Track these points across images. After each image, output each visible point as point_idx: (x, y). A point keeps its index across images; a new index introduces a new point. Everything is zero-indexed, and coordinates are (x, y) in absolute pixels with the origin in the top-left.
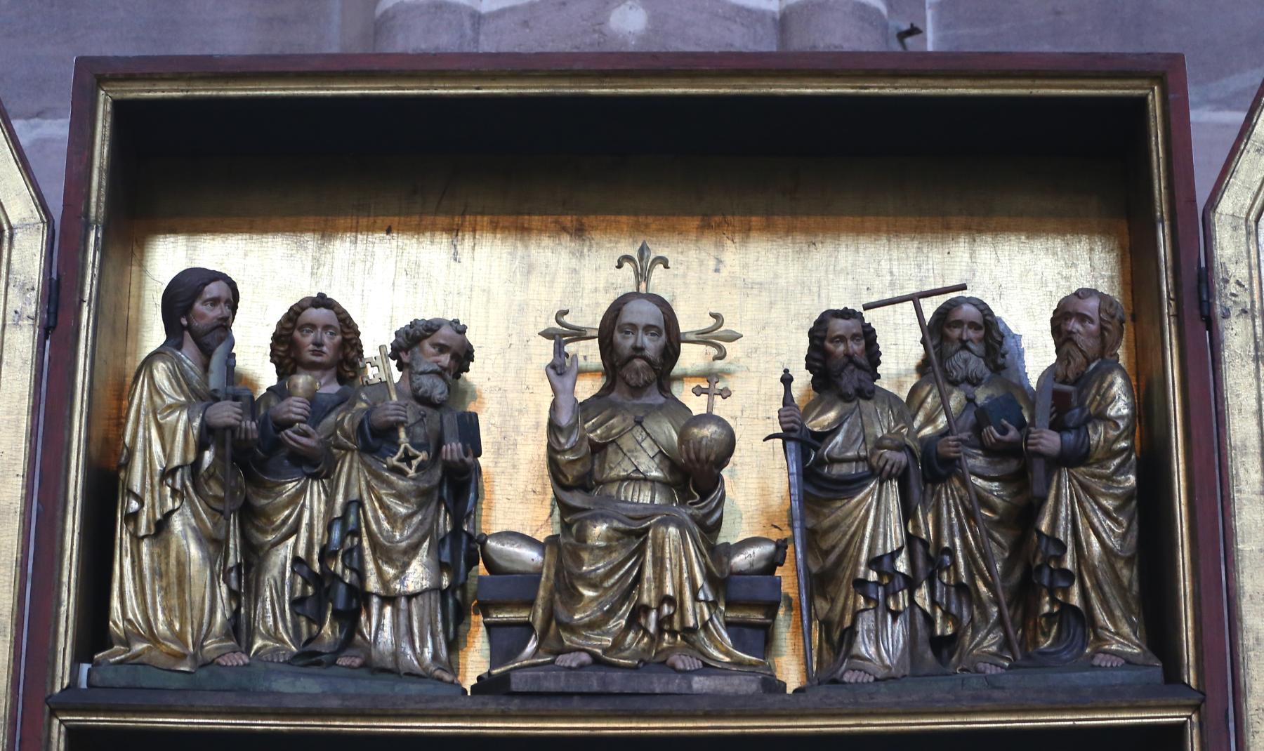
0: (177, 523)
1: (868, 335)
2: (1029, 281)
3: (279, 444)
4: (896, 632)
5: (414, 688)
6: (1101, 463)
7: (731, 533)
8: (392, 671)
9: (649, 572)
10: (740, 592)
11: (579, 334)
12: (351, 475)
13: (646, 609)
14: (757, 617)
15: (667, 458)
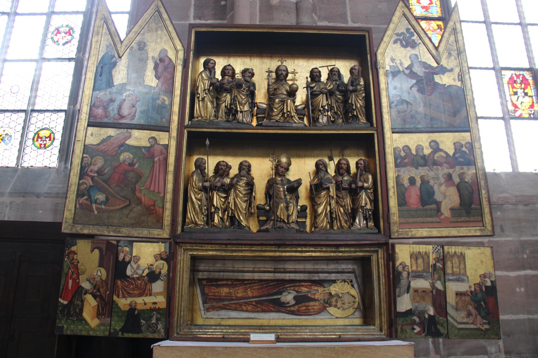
0: (206, 99)
1: (320, 72)
2: (345, 67)
3: (223, 87)
4: (325, 119)
5: (246, 125)
6: (359, 92)
7: (297, 103)
8: (243, 123)
9: (285, 107)
10: (299, 112)
11: (272, 72)
12: (235, 92)
13: (285, 113)
14: (302, 117)
15: (287, 91)
